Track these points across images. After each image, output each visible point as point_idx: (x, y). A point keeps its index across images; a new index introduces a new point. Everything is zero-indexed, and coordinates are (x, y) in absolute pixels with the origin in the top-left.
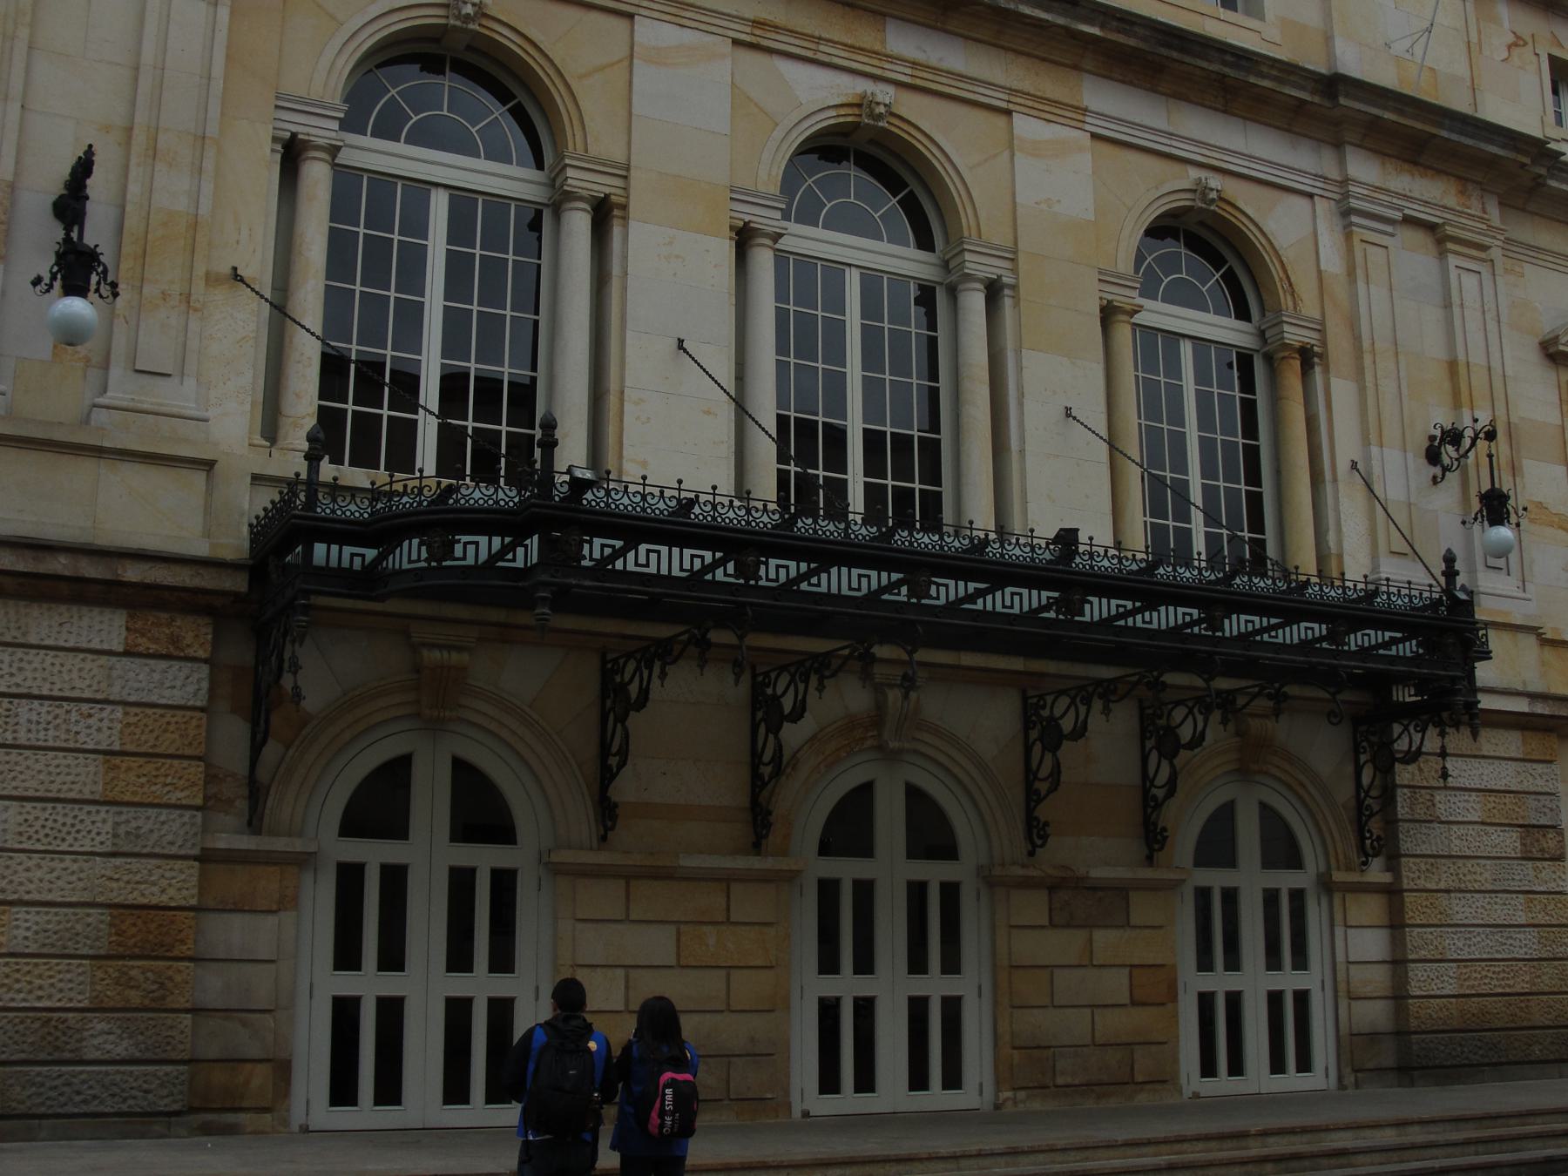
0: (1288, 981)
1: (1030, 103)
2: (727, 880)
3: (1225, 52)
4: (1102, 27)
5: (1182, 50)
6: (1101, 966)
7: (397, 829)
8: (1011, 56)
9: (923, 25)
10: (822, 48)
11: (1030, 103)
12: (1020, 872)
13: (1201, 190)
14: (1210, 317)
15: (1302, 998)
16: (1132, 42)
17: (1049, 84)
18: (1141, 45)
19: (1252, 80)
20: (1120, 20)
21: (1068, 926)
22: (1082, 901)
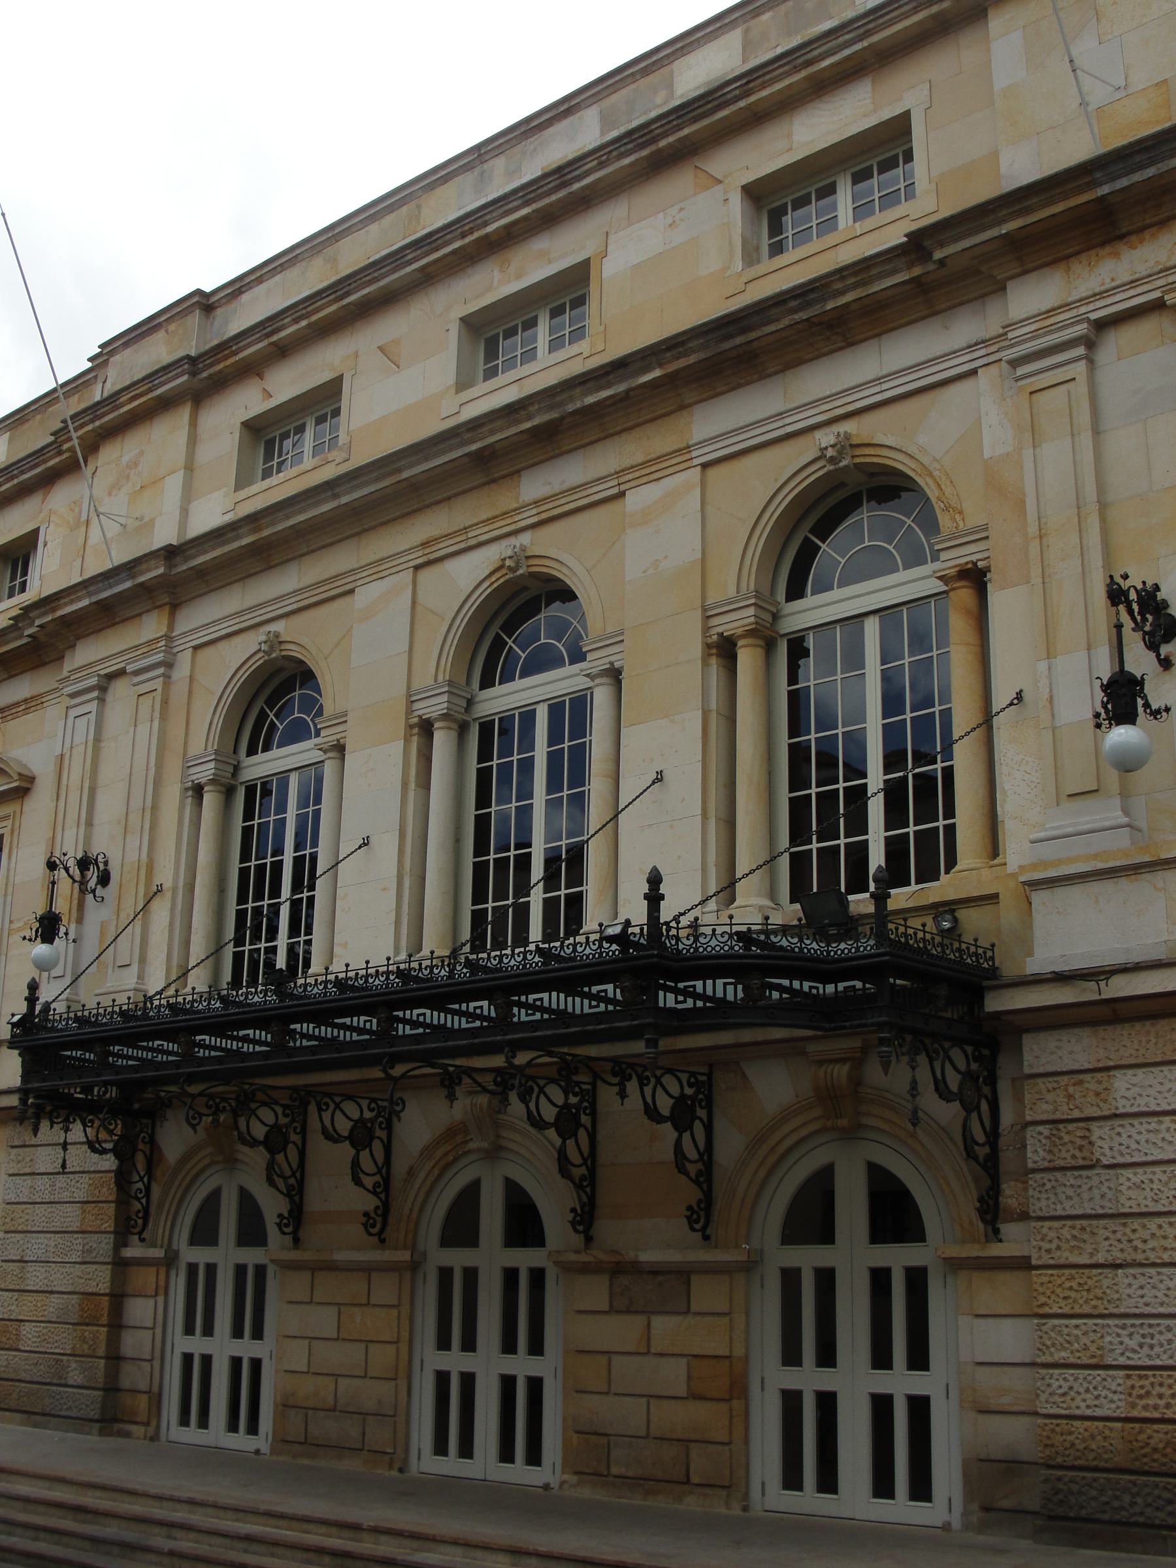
0: (522, 1366)
1: (637, 474)
2: (368, 1270)
3: (784, 302)
4: (660, 365)
5: (744, 331)
6: (661, 1355)
7: (827, 1236)
8: (625, 436)
9: (542, 462)
10: (470, 535)
11: (637, 474)
12: (573, 1257)
13: (846, 445)
14: (902, 575)
15: (535, 1386)
16: (692, 359)
17: (658, 440)
18: (703, 355)
19: (830, 305)
20: (669, 349)
21: (628, 1311)
22: (645, 1288)
